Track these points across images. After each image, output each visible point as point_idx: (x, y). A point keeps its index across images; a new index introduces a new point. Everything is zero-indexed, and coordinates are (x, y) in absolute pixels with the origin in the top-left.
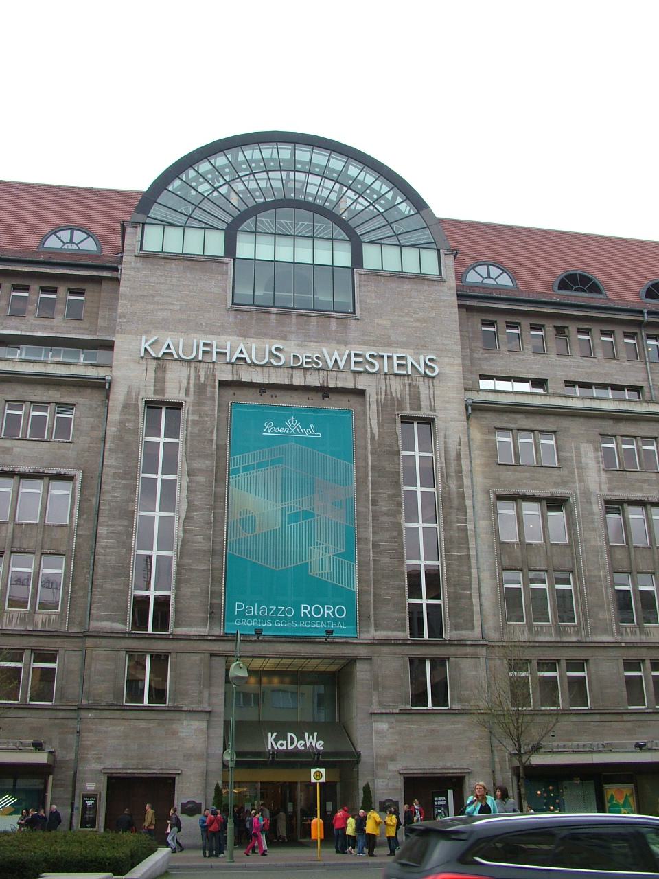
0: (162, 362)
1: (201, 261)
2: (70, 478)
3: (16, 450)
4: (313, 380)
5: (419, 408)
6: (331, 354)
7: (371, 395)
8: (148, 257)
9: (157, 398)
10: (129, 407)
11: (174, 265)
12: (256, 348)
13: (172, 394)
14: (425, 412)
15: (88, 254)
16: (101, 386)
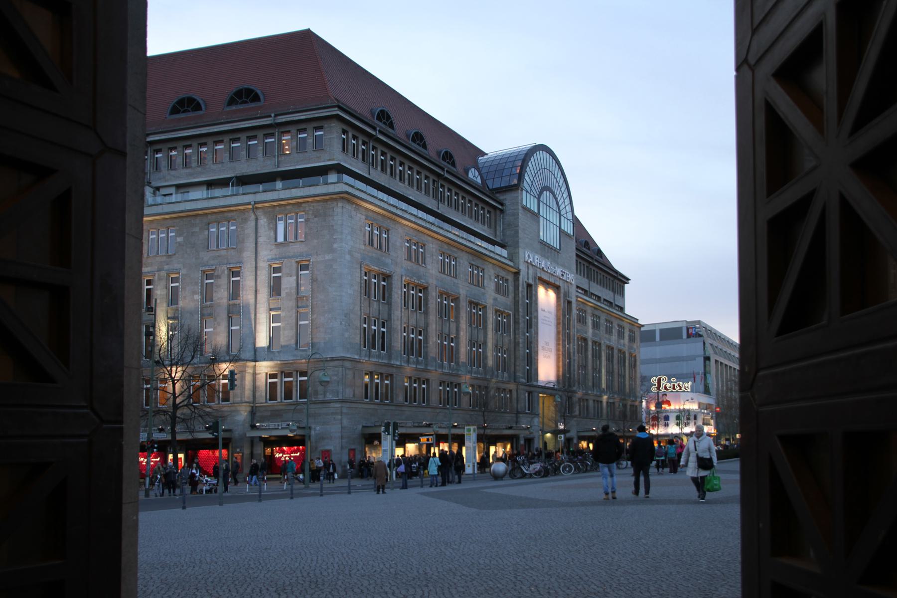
0: (529, 264)
1: (532, 212)
2: (509, 315)
3: (498, 299)
4: (552, 280)
5: (569, 297)
6: (558, 271)
7: (562, 288)
8: (525, 209)
9: (527, 281)
10: (523, 285)
11: (529, 215)
12: (544, 263)
13: (531, 281)
14: (569, 299)
15: (477, 183)
16: (517, 274)
